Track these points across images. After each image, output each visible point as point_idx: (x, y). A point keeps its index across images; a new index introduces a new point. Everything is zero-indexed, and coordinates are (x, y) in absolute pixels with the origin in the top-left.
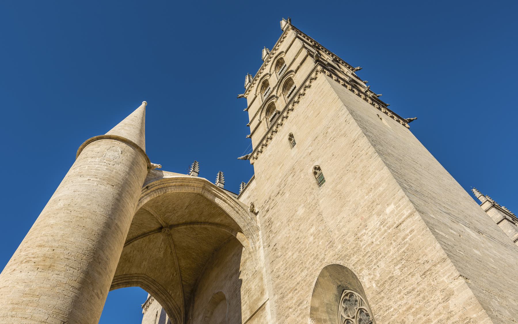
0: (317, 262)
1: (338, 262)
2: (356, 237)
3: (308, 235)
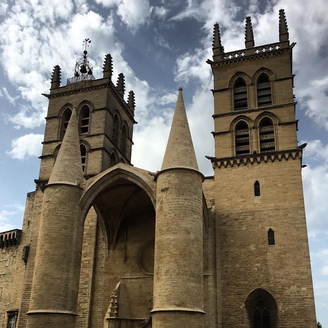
0: (256, 283)
1: (269, 291)
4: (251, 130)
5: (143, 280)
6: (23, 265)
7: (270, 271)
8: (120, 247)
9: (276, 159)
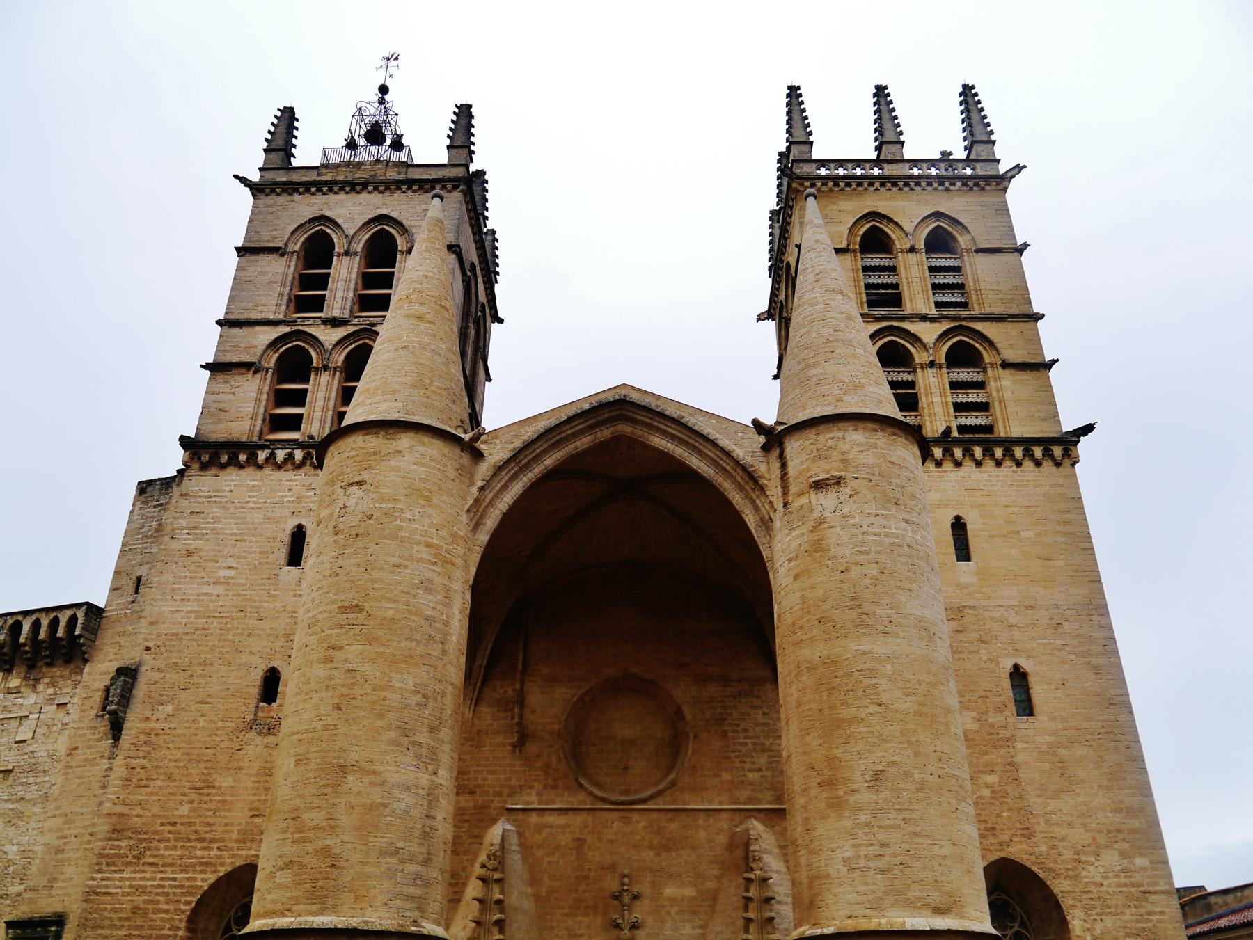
0: (991, 840)
1: (1035, 869)
2: (1077, 857)
3: (980, 781)
4: (922, 368)
5: (590, 818)
6: (99, 740)
7: (1032, 800)
8: (498, 696)
9: (1007, 458)
